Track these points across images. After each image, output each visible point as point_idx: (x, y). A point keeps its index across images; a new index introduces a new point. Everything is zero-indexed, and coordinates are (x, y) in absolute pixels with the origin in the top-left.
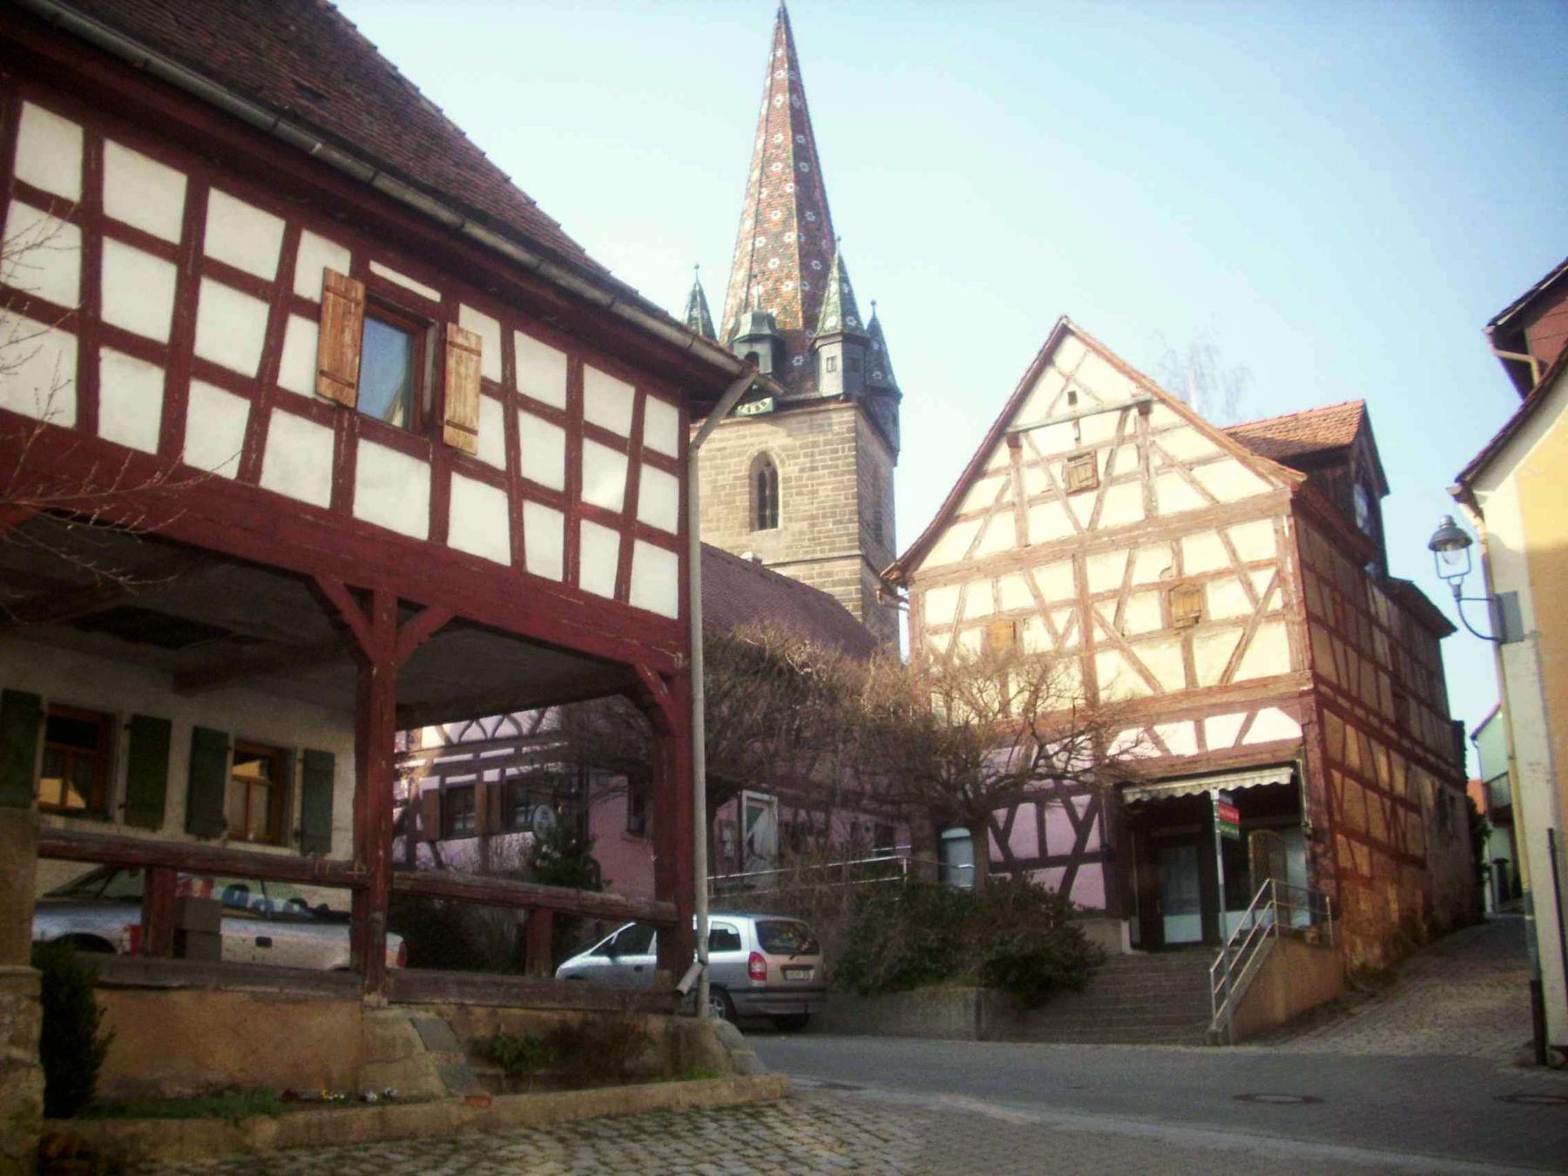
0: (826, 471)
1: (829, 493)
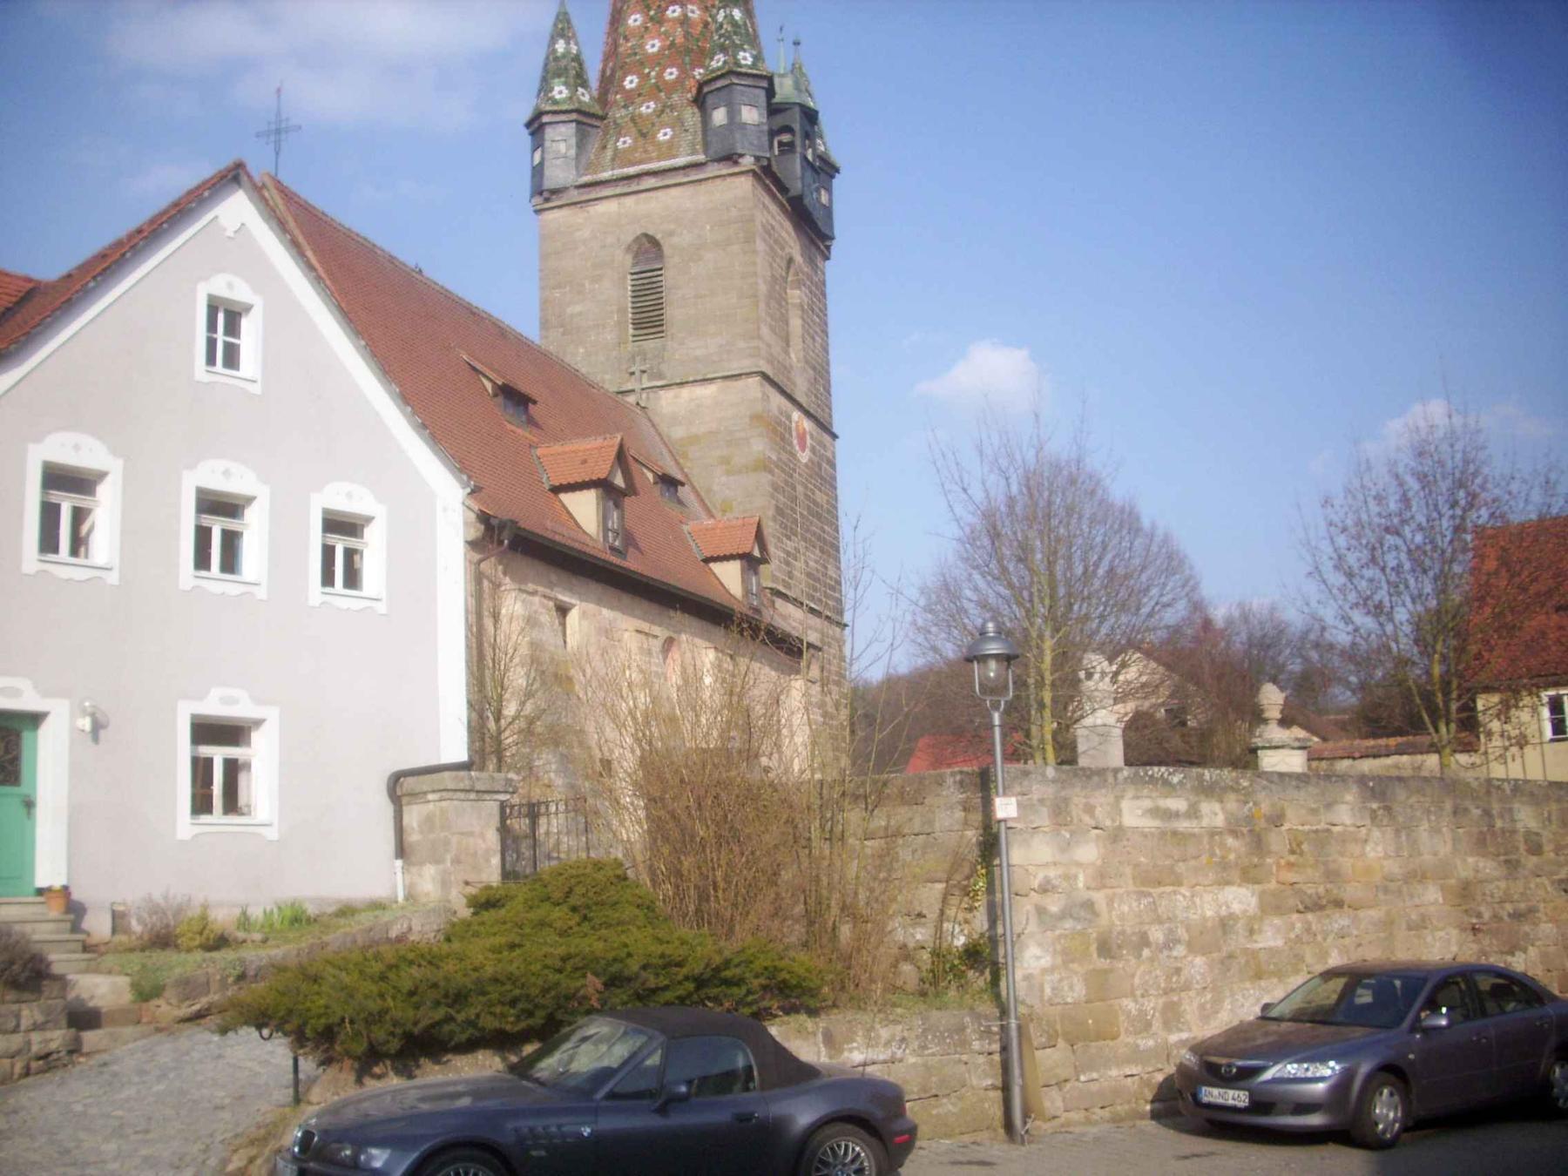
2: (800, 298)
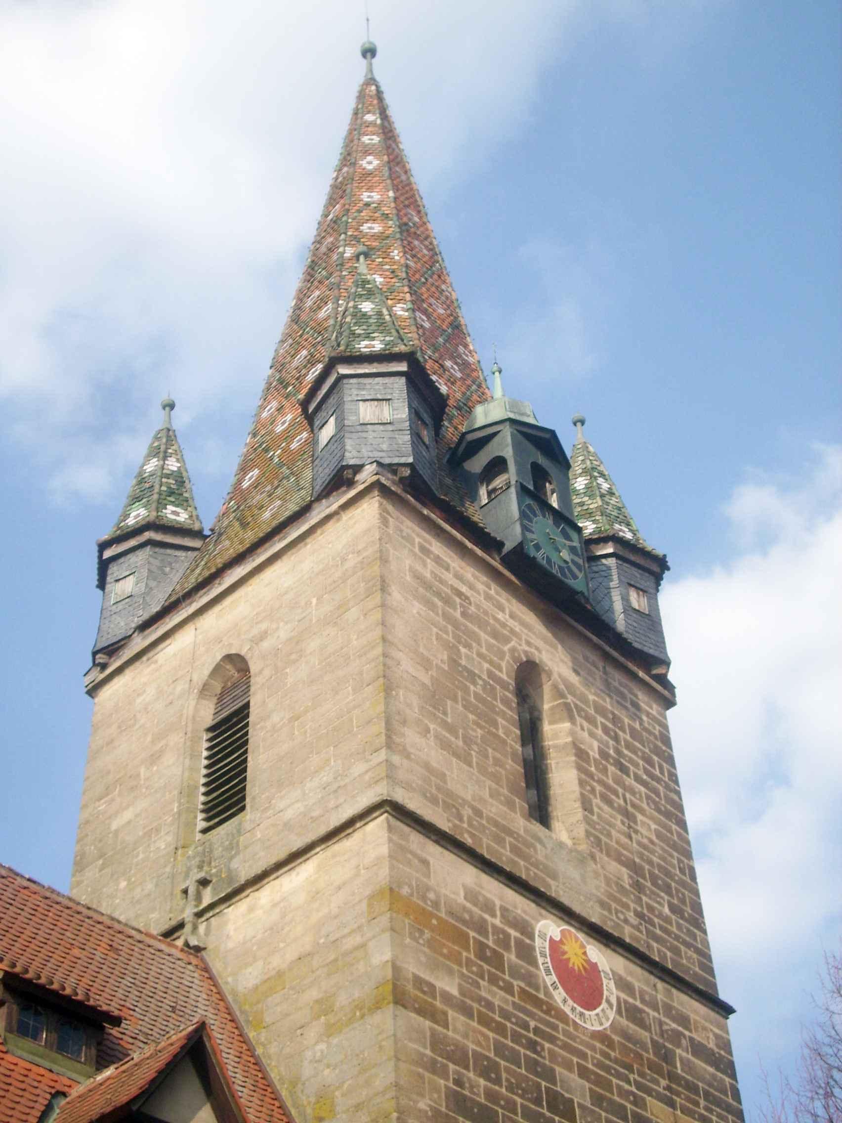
0: (643, 789)
1: (654, 838)
2: (572, 733)
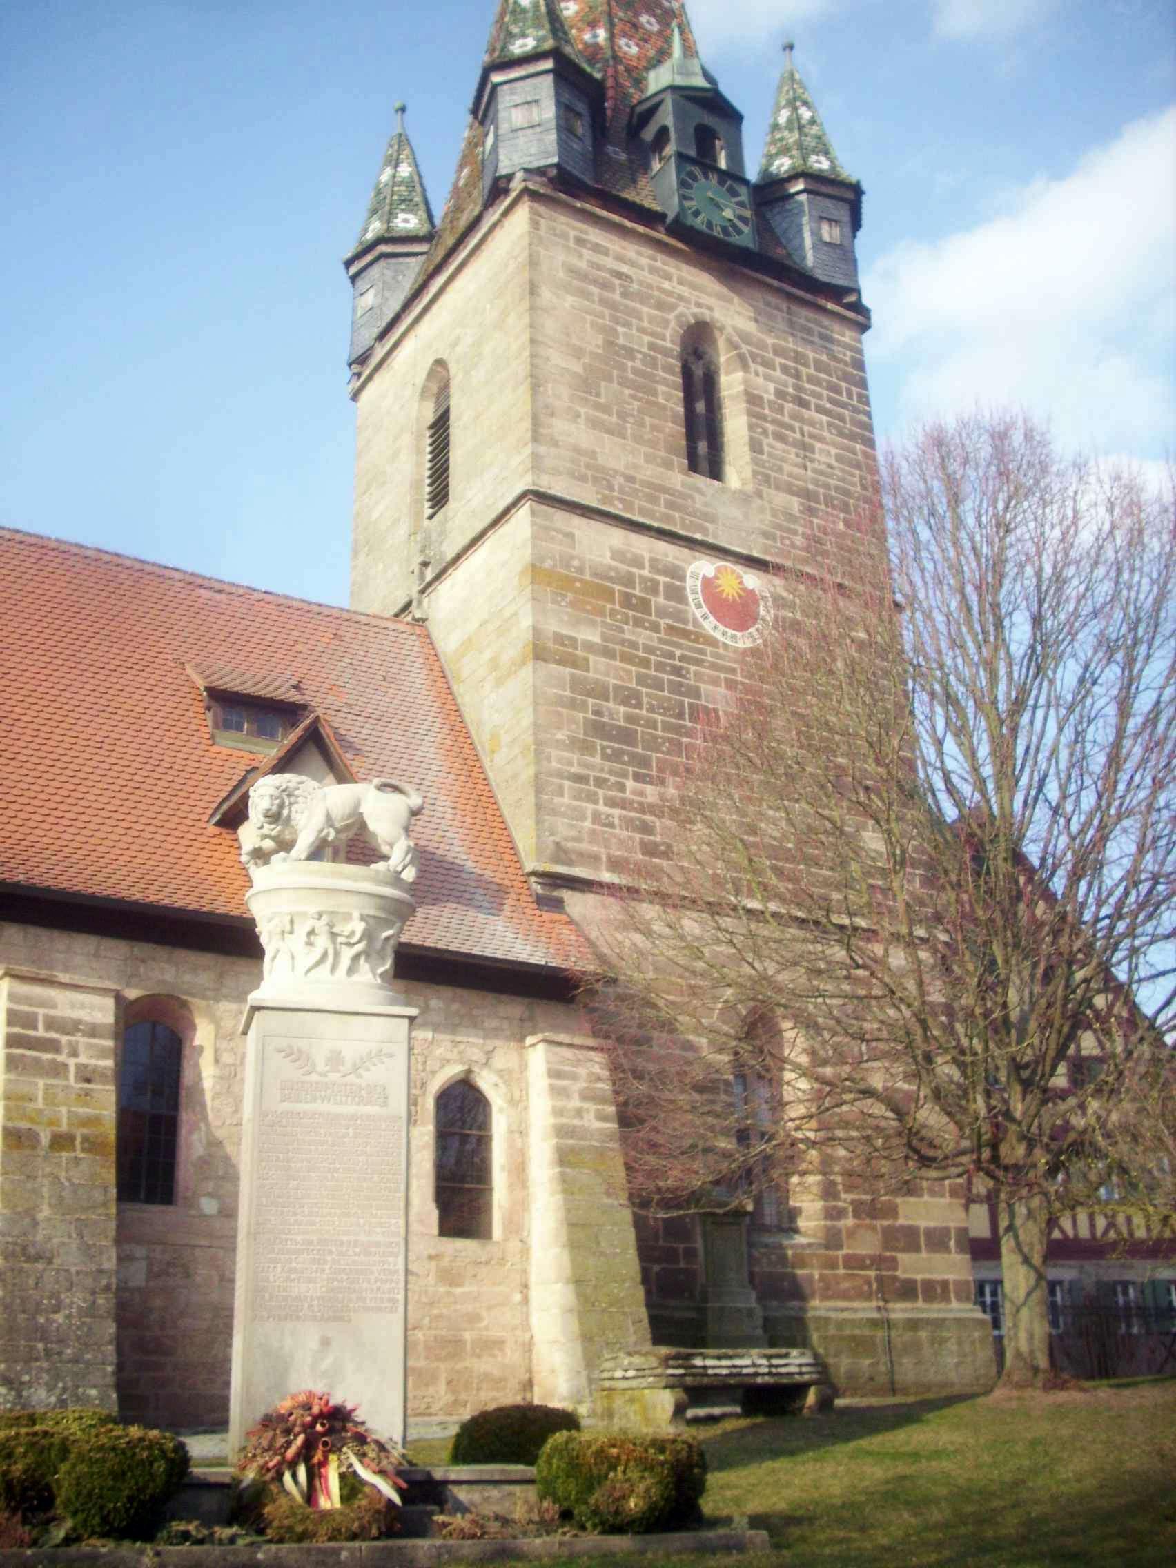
0: (825, 418)
1: (833, 462)
2: (746, 382)
